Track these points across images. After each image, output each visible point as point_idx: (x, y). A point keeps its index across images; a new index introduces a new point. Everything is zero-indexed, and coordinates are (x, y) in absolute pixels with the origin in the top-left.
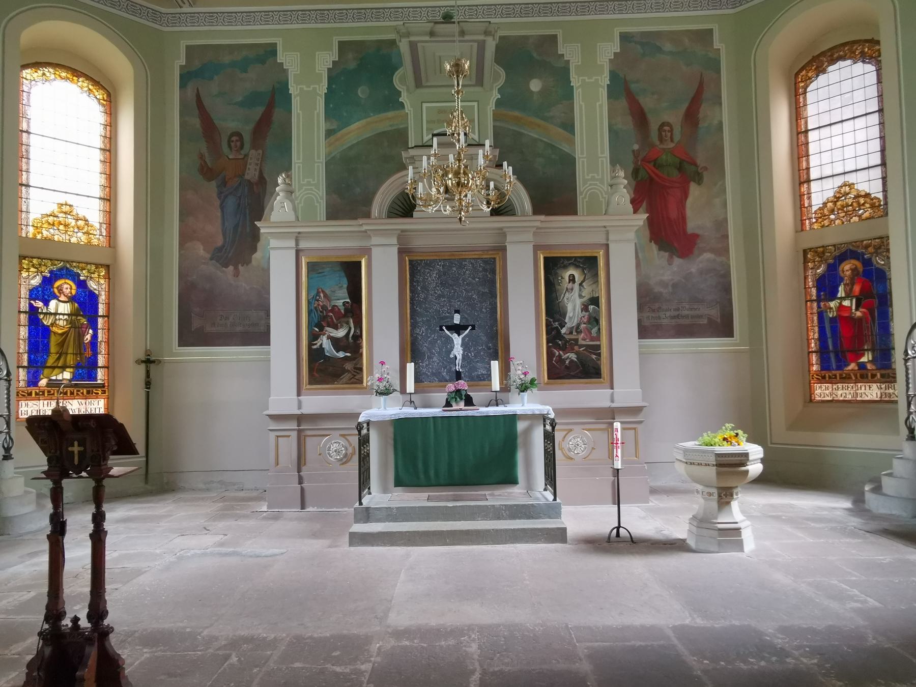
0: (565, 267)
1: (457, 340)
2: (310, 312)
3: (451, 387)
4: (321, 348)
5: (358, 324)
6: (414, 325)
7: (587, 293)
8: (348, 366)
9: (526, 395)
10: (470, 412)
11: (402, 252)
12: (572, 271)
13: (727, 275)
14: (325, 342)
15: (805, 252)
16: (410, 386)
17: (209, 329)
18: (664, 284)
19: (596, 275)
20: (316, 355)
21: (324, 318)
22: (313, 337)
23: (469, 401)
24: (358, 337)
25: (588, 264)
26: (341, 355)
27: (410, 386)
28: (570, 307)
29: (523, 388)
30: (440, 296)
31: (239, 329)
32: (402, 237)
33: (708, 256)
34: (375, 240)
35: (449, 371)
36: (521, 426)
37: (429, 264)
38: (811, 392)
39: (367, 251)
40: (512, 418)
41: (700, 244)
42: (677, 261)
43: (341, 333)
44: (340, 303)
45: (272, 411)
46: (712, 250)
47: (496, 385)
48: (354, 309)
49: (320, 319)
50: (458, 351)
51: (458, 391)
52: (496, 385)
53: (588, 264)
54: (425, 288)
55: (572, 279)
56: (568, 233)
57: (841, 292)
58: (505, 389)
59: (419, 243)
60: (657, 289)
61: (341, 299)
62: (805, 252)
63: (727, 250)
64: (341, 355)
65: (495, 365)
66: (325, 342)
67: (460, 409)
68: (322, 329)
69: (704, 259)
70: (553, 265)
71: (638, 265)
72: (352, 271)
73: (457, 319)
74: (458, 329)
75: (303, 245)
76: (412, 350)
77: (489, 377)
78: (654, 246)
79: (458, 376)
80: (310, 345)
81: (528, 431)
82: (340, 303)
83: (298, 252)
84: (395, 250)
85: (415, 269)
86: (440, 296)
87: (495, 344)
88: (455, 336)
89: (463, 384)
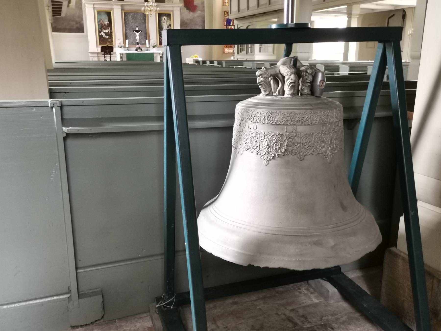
0: (163, 16)
1: (137, 34)
2: (98, 25)
3: (137, 46)
4: (102, 35)
5: (111, 29)
6: (126, 30)
7: (168, 24)
8: (109, 40)
9: (154, 48)
10: (142, 52)
11: (122, 10)
12: (165, 17)
13: (204, 18)
14: (103, 33)
15: (224, 12)
16: (127, 46)
17: (58, 27)
18: (187, 19)
19: (170, 19)
20: (101, 37)
21: (102, 27)
22: (100, 32)
23: (141, 50)
24: (111, 32)
25: (169, 16)
26: (107, 37)
27: (127, 46)
28: (164, 27)
29: (154, 47)
30: (133, 22)
31: (68, 27)
32: (122, 6)
33: (199, 12)
34: (114, 6)
35: (135, 42)
36: (155, 55)
37: (129, 13)
38: (224, 50)
39: (112, 9)
40: (152, 54)
41: (198, 9)
42: (191, 13)
43: (107, 31)
44: (106, 23)
45: (90, 51)
46: (200, 11)
47: (148, 46)
48: (110, 25)
49: (101, 27)
50: (138, 37)
51: (139, 47)
52: (148, 46)
53: (169, 16)
54: (128, 20)
55: (165, 19)
56: (164, 8)
57: (231, 24)
58: (149, 47)
59: (126, 8)
60: (186, 21)
61: (106, 22)
62: (224, 12)
63: (204, 11)
64: (107, 37)
65: (147, 41)
66: (103, 33)
67: (139, 51)
68: (102, 30)
69: (198, 13)
70: (160, 15)
71: (181, 14)
72: (109, 14)
73: (137, 29)
74: (137, 31)
75: (95, 6)
76: (126, 37)
77: (145, 44)
78: (185, 8)
79: (138, 44)
80: (99, 34)
81: (156, 56)
82: (106, 23)
83: (94, 8)
84: (120, 10)
85: (126, 15)
86: (133, 22)
87: (146, 36)
88: (137, 33)
89: (140, 45)
